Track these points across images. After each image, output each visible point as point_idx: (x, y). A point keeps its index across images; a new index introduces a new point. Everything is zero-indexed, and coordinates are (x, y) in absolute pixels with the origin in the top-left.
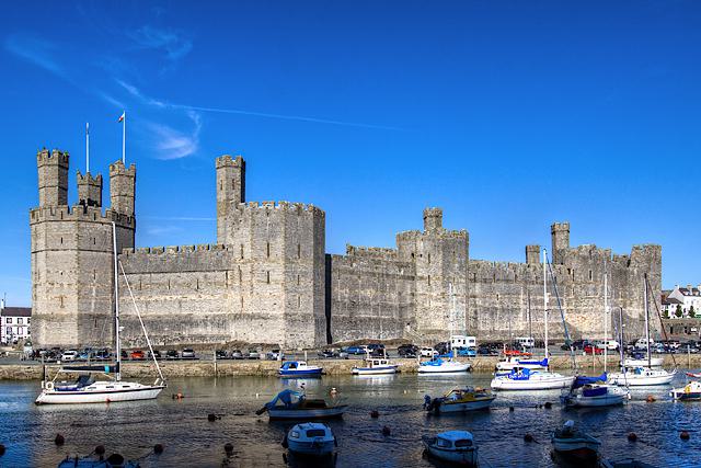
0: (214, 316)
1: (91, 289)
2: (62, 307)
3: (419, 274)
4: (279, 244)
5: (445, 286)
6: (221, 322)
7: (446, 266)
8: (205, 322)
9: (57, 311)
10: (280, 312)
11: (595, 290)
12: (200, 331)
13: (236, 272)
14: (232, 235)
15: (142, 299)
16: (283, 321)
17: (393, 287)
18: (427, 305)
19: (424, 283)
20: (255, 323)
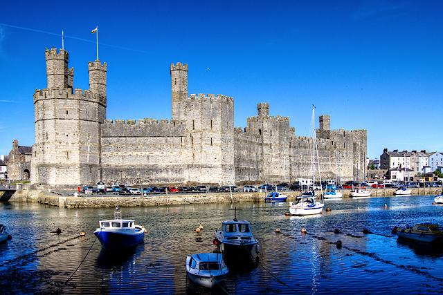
0: (173, 166)
1: (87, 147)
2: (68, 158)
3: (265, 142)
4: (218, 121)
5: (281, 149)
6: (178, 170)
7: (281, 138)
8: (167, 169)
9: (64, 161)
10: (219, 164)
11: (346, 153)
12: (164, 175)
13: (189, 138)
14: (185, 114)
15: (119, 154)
16: (221, 169)
17: (254, 150)
18: (269, 161)
19: (268, 147)
20: (204, 170)
